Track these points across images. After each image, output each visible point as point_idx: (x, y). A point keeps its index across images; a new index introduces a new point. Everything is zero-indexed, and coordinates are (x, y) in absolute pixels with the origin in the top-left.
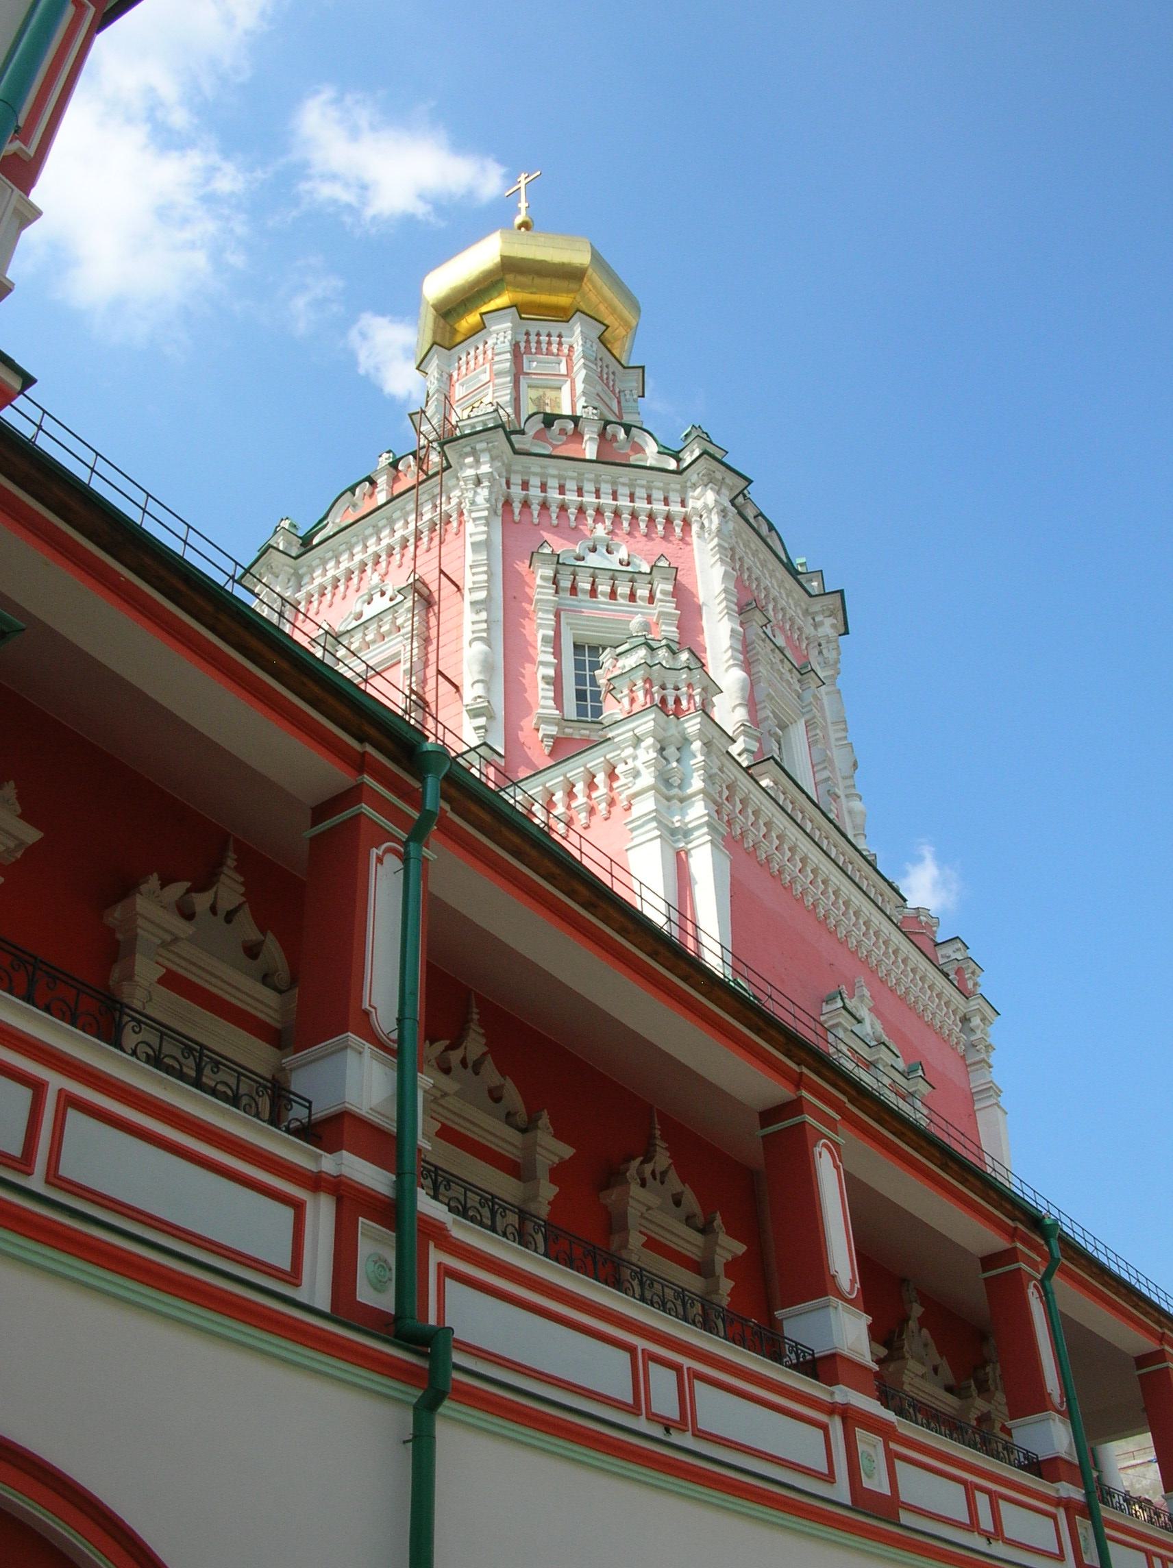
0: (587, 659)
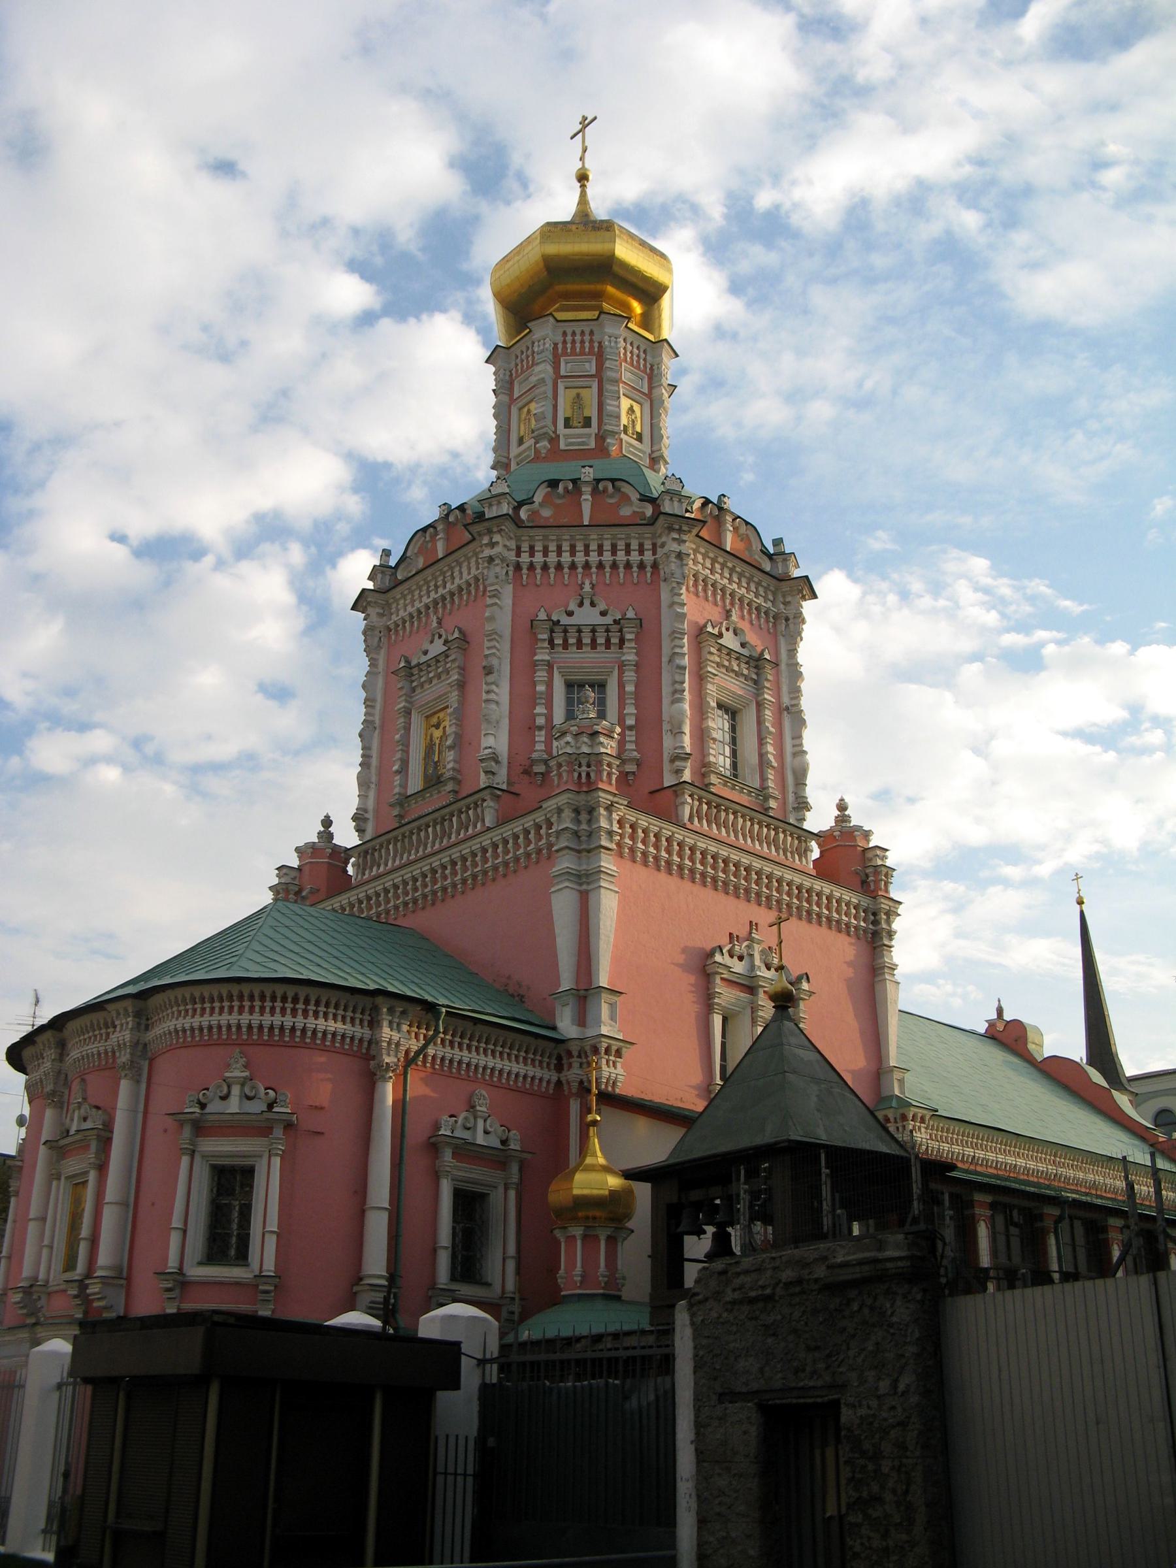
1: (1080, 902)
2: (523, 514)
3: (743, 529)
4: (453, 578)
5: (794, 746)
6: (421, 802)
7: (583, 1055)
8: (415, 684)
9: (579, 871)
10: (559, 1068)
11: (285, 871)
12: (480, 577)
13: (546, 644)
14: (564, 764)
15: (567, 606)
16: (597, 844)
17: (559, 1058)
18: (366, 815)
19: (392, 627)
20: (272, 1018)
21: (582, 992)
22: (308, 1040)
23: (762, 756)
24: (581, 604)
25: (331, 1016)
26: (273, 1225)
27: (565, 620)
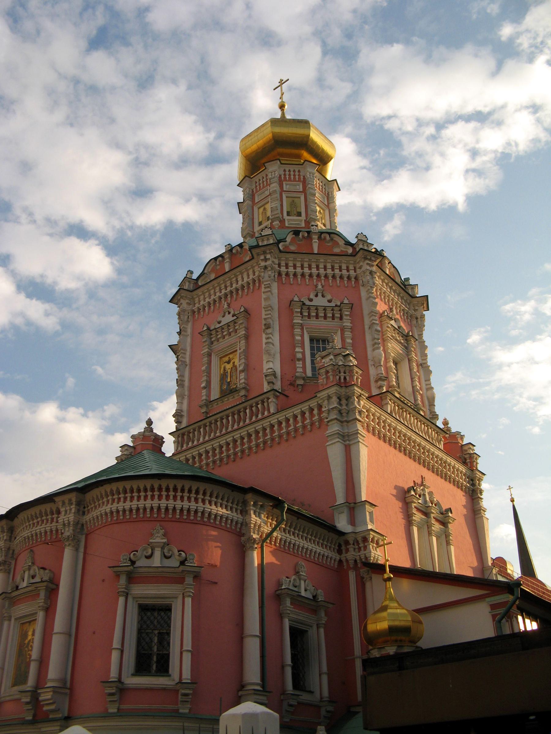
0: (315, 345)
1: (512, 500)
2: (281, 246)
3: (393, 269)
4: (237, 282)
5: (426, 385)
6: (221, 404)
7: (356, 544)
8: (213, 340)
9: (343, 433)
10: (340, 552)
11: (126, 448)
12: (256, 279)
13: (299, 315)
14: (330, 371)
15: (309, 296)
16: (354, 417)
17: (340, 546)
18: (182, 413)
19: (196, 310)
20: (182, 503)
21: (352, 505)
22: (206, 520)
23: (413, 387)
24: (316, 296)
25: (219, 505)
26: (188, 645)
27: (308, 303)
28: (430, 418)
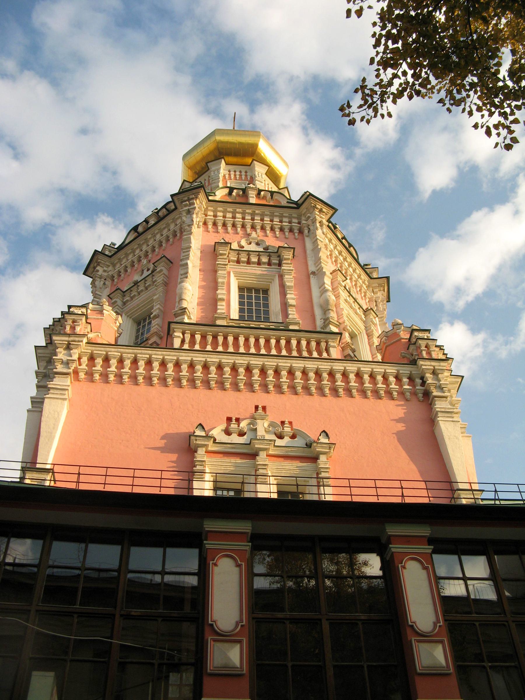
28: (322, 328)
